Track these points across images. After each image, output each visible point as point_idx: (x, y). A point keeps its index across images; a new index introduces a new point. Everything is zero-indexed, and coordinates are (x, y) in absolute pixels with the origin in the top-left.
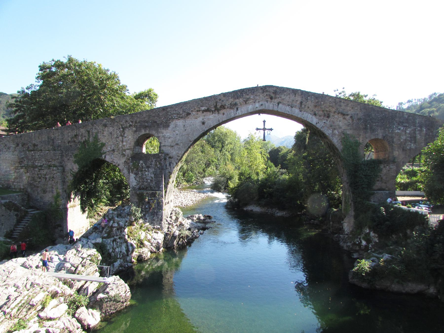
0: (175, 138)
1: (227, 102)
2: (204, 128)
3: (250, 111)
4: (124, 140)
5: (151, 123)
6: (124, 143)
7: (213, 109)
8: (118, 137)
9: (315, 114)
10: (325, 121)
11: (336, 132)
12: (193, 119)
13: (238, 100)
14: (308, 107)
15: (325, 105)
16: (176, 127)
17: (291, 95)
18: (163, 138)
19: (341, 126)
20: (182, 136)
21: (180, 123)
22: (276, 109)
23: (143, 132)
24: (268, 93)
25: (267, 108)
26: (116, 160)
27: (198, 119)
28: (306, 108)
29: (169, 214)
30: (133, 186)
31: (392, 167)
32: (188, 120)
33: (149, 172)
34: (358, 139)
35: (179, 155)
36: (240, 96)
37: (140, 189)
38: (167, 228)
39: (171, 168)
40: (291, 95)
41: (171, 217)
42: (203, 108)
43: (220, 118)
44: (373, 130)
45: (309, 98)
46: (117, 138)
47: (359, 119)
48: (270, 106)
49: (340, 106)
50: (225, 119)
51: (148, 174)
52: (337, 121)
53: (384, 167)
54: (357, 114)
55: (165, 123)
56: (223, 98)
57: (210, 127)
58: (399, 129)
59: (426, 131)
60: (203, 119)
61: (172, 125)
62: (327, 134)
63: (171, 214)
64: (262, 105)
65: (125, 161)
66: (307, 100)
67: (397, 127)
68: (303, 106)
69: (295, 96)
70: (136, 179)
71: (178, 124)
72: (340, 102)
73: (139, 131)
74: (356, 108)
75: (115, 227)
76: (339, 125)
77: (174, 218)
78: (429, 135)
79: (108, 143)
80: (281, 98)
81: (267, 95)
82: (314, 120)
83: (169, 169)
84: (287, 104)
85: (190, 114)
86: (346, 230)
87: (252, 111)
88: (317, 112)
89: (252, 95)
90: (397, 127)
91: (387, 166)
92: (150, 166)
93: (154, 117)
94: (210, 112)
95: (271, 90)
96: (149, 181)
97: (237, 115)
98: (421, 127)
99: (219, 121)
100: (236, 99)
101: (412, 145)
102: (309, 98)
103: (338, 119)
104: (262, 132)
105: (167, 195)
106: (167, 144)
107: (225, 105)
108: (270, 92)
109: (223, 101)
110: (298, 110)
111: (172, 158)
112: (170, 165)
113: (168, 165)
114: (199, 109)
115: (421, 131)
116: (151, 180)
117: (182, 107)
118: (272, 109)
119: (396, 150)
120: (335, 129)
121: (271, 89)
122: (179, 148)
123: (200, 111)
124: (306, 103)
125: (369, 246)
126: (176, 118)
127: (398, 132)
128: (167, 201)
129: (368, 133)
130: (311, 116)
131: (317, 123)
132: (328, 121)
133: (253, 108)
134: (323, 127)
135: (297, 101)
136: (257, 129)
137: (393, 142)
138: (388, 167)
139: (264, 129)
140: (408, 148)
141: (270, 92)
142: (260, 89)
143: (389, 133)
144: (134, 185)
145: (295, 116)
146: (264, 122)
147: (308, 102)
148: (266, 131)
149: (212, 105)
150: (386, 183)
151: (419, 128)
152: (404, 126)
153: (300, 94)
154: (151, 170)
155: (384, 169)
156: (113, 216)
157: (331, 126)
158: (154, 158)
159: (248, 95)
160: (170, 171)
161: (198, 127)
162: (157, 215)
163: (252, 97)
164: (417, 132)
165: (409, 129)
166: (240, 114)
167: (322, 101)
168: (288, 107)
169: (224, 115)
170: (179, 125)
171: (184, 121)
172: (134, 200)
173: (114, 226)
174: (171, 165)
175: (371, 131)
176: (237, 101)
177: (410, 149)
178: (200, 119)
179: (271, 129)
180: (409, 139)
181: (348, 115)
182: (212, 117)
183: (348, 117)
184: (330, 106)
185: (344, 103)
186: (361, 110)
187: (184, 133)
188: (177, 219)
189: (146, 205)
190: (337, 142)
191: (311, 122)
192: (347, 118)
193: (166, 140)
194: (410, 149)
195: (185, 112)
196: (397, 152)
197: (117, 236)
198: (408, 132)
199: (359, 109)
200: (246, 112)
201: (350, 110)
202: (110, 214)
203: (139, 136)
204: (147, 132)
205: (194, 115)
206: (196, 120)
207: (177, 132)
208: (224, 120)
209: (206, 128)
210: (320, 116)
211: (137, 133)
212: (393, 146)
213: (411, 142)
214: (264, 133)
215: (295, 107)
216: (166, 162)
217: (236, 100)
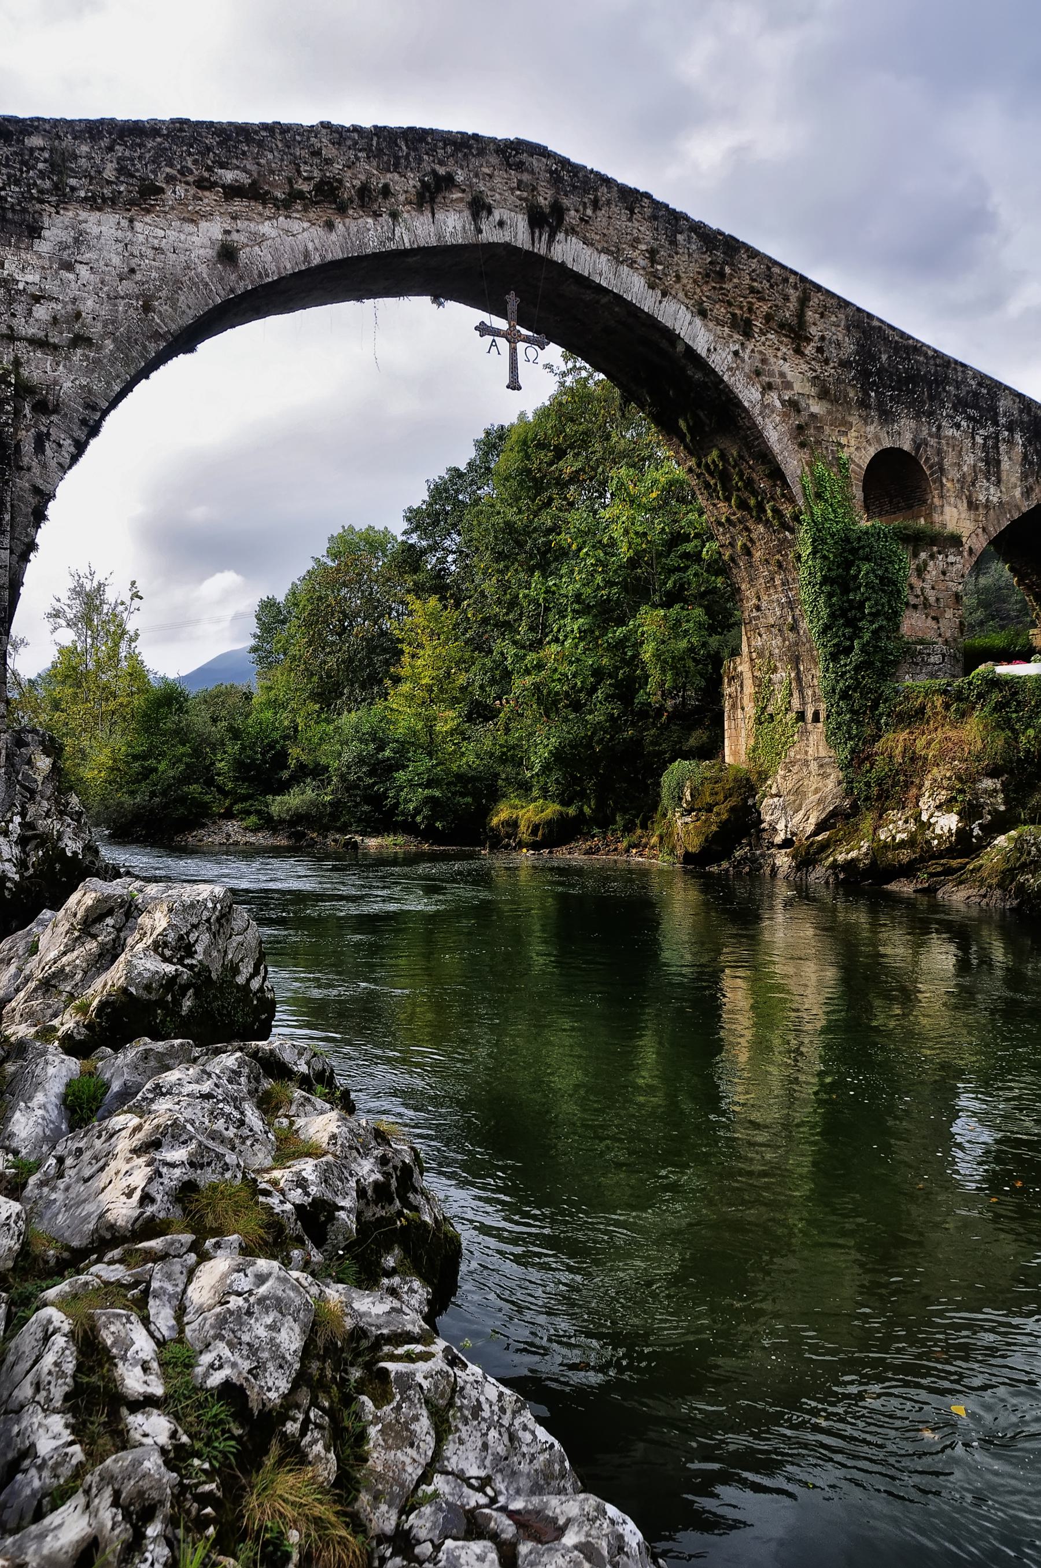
0: (74, 301)
1: (349, 174)
2: (233, 277)
3: (450, 240)
7: (279, 195)
9: (703, 313)
10: (737, 347)
11: (773, 398)
12: (176, 224)
13: (396, 176)
14: (678, 278)
15: (736, 280)
16: (76, 240)
17: (617, 210)
19: (789, 378)
20: (113, 298)
24: (526, 177)
27: (203, 225)
28: (670, 280)
32: (148, 219)
34: (843, 440)
36: (407, 157)
39: (44, 466)
41: (29, 762)
42: (229, 176)
43: (310, 246)
44: (887, 417)
45: (679, 237)
47: (844, 364)
49: (786, 298)
52: (776, 356)
53: (932, 557)
54: (838, 345)
55: (14, 211)
56: (329, 151)
57: (260, 275)
58: (958, 426)
60: (227, 232)
61: (55, 231)
62: (746, 404)
64: (501, 224)
66: (673, 242)
67: (952, 417)
68: (660, 267)
71: (95, 230)
72: (786, 280)
74: (833, 319)
76: (782, 375)
78: (1031, 463)
81: (520, 182)
83: (36, 470)
85: (161, 191)
86: (781, 826)
90: (952, 417)
91: (940, 553)
94: (264, 204)
98: (1010, 429)
99: (307, 255)
100: (389, 171)
101: (992, 490)
102: (679, 237)
103: (778, 349)
104: (503, 343)
107: (340, 181)
108: (532, 172)
109: (328, 162)
110: (643, 281)
111: (56, 410)
112: (39, 448)
113: (28, 447)
114: (206, 174)
115: (1010, 442)
117: (110, 149)
119: (952, 500)
120: (768, 387)
121: (539, 161)
122: (97, 362)
123: (214, 184)
125: (972, 830)
126: (82, 194)
129: (872, 422)
130: (689, 316)
131: (709, 350)
132: (748, 351)
133: (464, 227)
135: (637, 240)
137: (942, 470)
138: (940, 557)
141: (532, 172)
142: (492, 146)
143: (930, 435)
145: (630, 302)
147: (677, 253)
149: (272, 172)
150: (934, 618)
152: (970, 418)
153: (648, 211)
157: (758, 373)
159: (441, 163)
160: (39, 482)
161: (203, 269)
163: (460, 177)
164: (1003, 447)
165: (981, 432)
166: (408, 246)
168: (604, 257)
169: (333, 237)
170: (98, 238)
171: (125, 223)
174: (49, 452)
175: (880, 417)
176: (391, 178)
177: (987, 506)
178: (213, 230)
180: (981, 464)
181: (808, 340)
182: (274, 233)
183: (809, 350)
184: (753, 290)
185: (795, 288)
186: (847, 328)
187: (126, 287)
190: (780, 440)
191: (690, 343)
192: (807, 352)
193: (19, 309)
194: (987, 506)
195: (133, 176)
198: (979, 440)
199: (843, 323)
201: (815, 324)
205: (181, 202)
206: (190, 228)
207: (83, 271)
208: (329, 257)
209: (241, 278)
210: (719, 323)
212: (942, 485)
213: (988, 480)
214: (513, 352)
215: (631, 266)
217: (389, 175)
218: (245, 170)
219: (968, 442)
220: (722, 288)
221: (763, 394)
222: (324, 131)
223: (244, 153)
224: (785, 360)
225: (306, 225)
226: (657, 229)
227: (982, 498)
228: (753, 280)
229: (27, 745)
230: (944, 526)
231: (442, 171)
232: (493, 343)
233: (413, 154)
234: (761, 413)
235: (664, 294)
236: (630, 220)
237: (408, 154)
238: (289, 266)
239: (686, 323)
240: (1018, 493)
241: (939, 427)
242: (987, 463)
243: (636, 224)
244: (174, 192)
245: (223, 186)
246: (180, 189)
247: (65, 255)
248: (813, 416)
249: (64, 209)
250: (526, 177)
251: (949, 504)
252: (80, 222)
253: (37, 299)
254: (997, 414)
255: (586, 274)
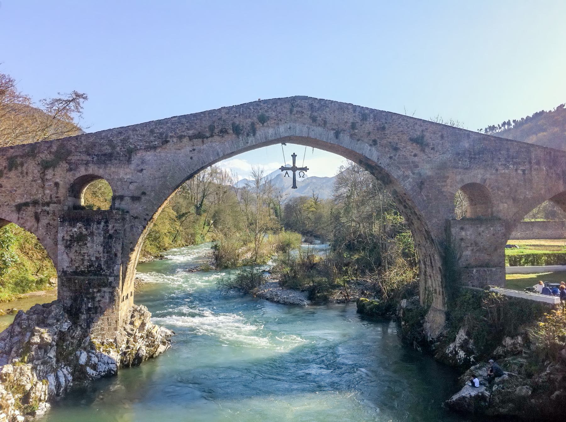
3: (270, 139)
4: (46, 186)
5: (97, 155)
6: (47, 192)
7: (208, 135)
8: (35, 181)
16: (142, 163)
18: (119, 183)
21: (149, 156)
22: (312, 135)
23: (82, 172)
24: (300, 109)
25: (298, 133)
26: (31, 222)
27: (183, 150)
29: (129, 317)
30: (63, 269)
31: (499, 229)
33: (93, 241)
35: (147, 212)
37: (75, 273)
38: (125, 342)
39: (133, 235)
40: (337, 113)
41: (132, 323)
42: (191, 132)
43: (219, 151)
46: (33, 183)
48: (300, 129)
50: (230, 152)
51: (92, 247)
57: (202, 164)
58: (508, 168)
59: (547, 170)
62: (396, 177)
63: (132, 316)
65: (49, 224)
69: (343, 115)
70: (68, 256)
73: (75, 170)
75: (35, 343)
77: (138, 323)
79: (16, 191)
80: (320, 117)
81: (297, 111)
82: (373, 154)
84: (331, 128)
85: (167, 142)
87: (273, 138)
88: (378, 141)
89: (274, 111)
92: (96, 231)
93: (103, 145)
95: (305, 104)
96: (93, 259)
97: (249, 145)
98: (538, 163)
99: (218, 154)
104: (290, 173)
105: (125, 284)
106: (126, 193)
113: (128, 230)
116: (97, 258)
118: (307, 136)
122: (149, 200)
123: (185, 136)
124: (361, 125)
127: (504, 173)
128: (125, 294)
130: (369, 148)
132: (397, 156)
133: (276, 134)
134: (388, 165)
135: (346, 122)
136: (283, 169)
138: (492, 229)
139: (294, 169)
140: (522, 197)
143: (491, 175)
144: (65, 267)
146: (294, 156)
148: (297, 172)
151: (536, 166)
153: (351, 111)
154: (99, 239)
155: (487, 232)
156: (29, 325)
158: (103, 219)
162: (108, 319)
164: (534, 173)
166: (254, 144)
167: (386, 123)
168: (332, 132)
172: (65, 294)
173: (33, 341)
174: (135, 230)
179: (306, 169)
180: (522, 183)
182: (207, 148)
188: (143, 324)
189: (89, 302)
190: (412, 189)
196: (505, 204)
197: (38, 359)
198: (520, 172)
200: (264, 140)
202: (24, 320)
203: (75, 178)
204: (90, 172)
206: (179, 151)
207: (144, 172)
211: (71, 173)
216: (124, 225)
217: (247, 120)
218: (195, 129)
219: (514, 174)
220: (384, 134)
221: (404, 172)
222: (222, 110)
223: (196, 123)
224: (415, 155)
225: (217, 144)
226: (355, 116)
227: (522, 197)
228: (400, 127)
229: (134, 317)
230: (499, 211)
231: (267, 115)
232: (287, 173)
233: (255, 111)
234: (403, 179)
235: (358, 140)
236: (343, 115)
237: (254, 111)
238: (212, 159)
239: (368, 151)
240: (543, 192)
241: (497, 170)
242: (525, 181)
243: (346, 117)
244: (173, 141)
245: (189, 136)
246: (175, 140)
247: (139, 168)
248: (429, 177)
249: (138, 153)
250: (300, 109)
251: (503, 203)
252: (143, 157)
253: (131, 183)
254: (531, 159)
255: (324, 140)
